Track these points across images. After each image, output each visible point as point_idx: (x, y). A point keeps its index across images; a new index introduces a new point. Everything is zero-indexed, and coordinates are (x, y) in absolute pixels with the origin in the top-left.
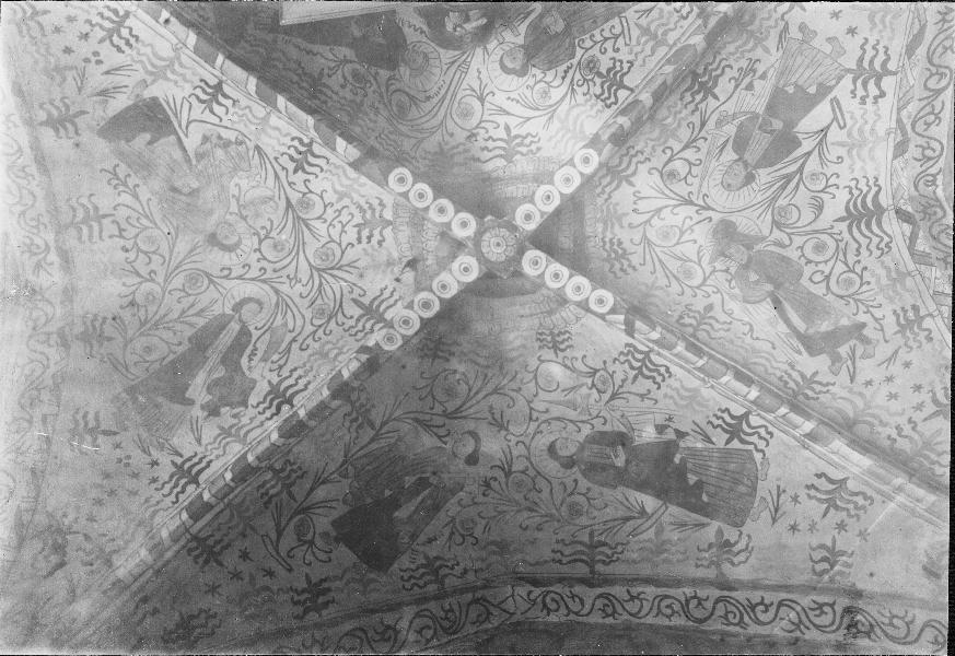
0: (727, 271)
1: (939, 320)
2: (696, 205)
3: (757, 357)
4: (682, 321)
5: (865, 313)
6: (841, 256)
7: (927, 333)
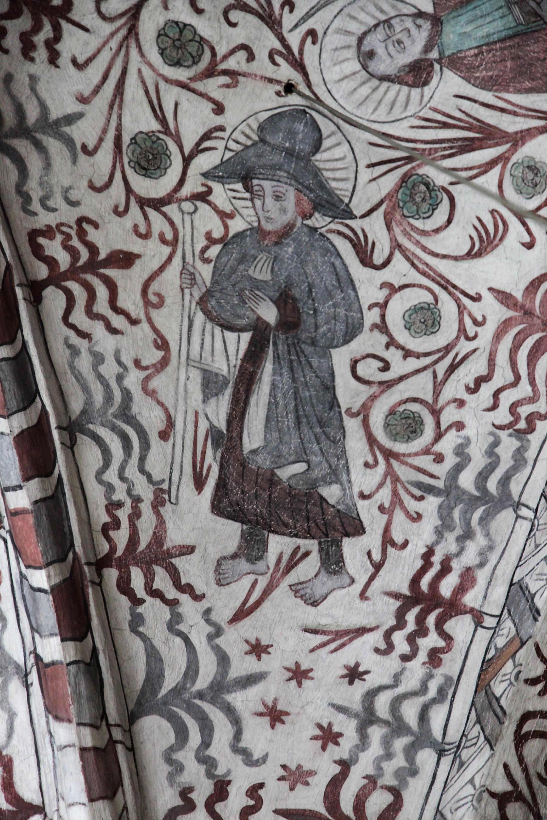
0: (224, 216)
1: (483, 635)
2: (282, 40)
3: (114, 428)
4: (41, 240)
5: (381, 509)
6: (442, 368)
7: (441, 643)
